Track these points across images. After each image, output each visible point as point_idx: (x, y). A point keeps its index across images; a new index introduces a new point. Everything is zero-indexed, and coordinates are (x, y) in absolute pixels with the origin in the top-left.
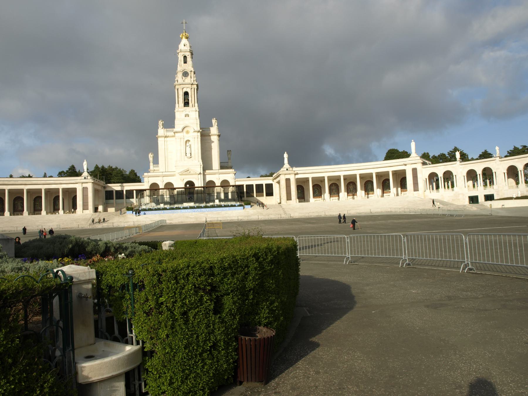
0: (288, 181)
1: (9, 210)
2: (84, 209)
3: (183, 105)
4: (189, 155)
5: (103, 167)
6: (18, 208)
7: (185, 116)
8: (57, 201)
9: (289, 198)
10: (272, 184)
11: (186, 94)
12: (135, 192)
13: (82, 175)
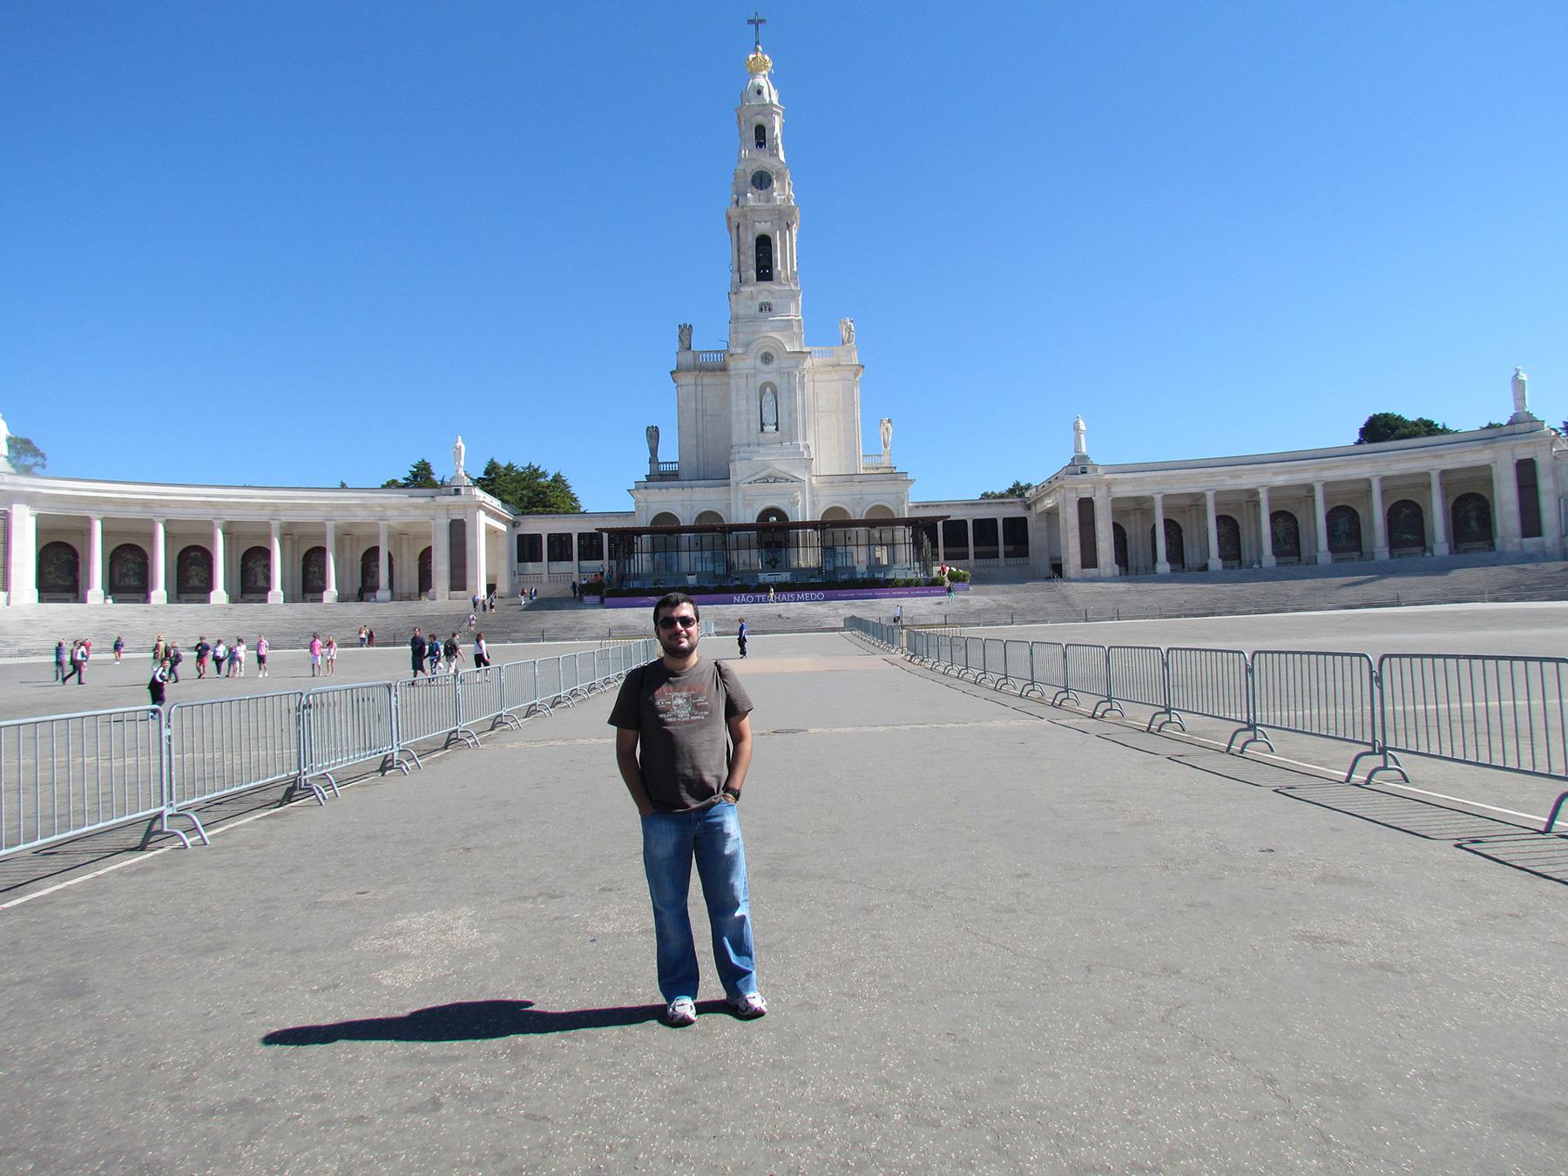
0: (1086, 507)
1: (228, 588)
3: (753, 273)
6: (256, 582)
7: (758, 307)
8: (374, 564)
9: (1089, 557)
10: (1024, 520)
12: (605, 535)
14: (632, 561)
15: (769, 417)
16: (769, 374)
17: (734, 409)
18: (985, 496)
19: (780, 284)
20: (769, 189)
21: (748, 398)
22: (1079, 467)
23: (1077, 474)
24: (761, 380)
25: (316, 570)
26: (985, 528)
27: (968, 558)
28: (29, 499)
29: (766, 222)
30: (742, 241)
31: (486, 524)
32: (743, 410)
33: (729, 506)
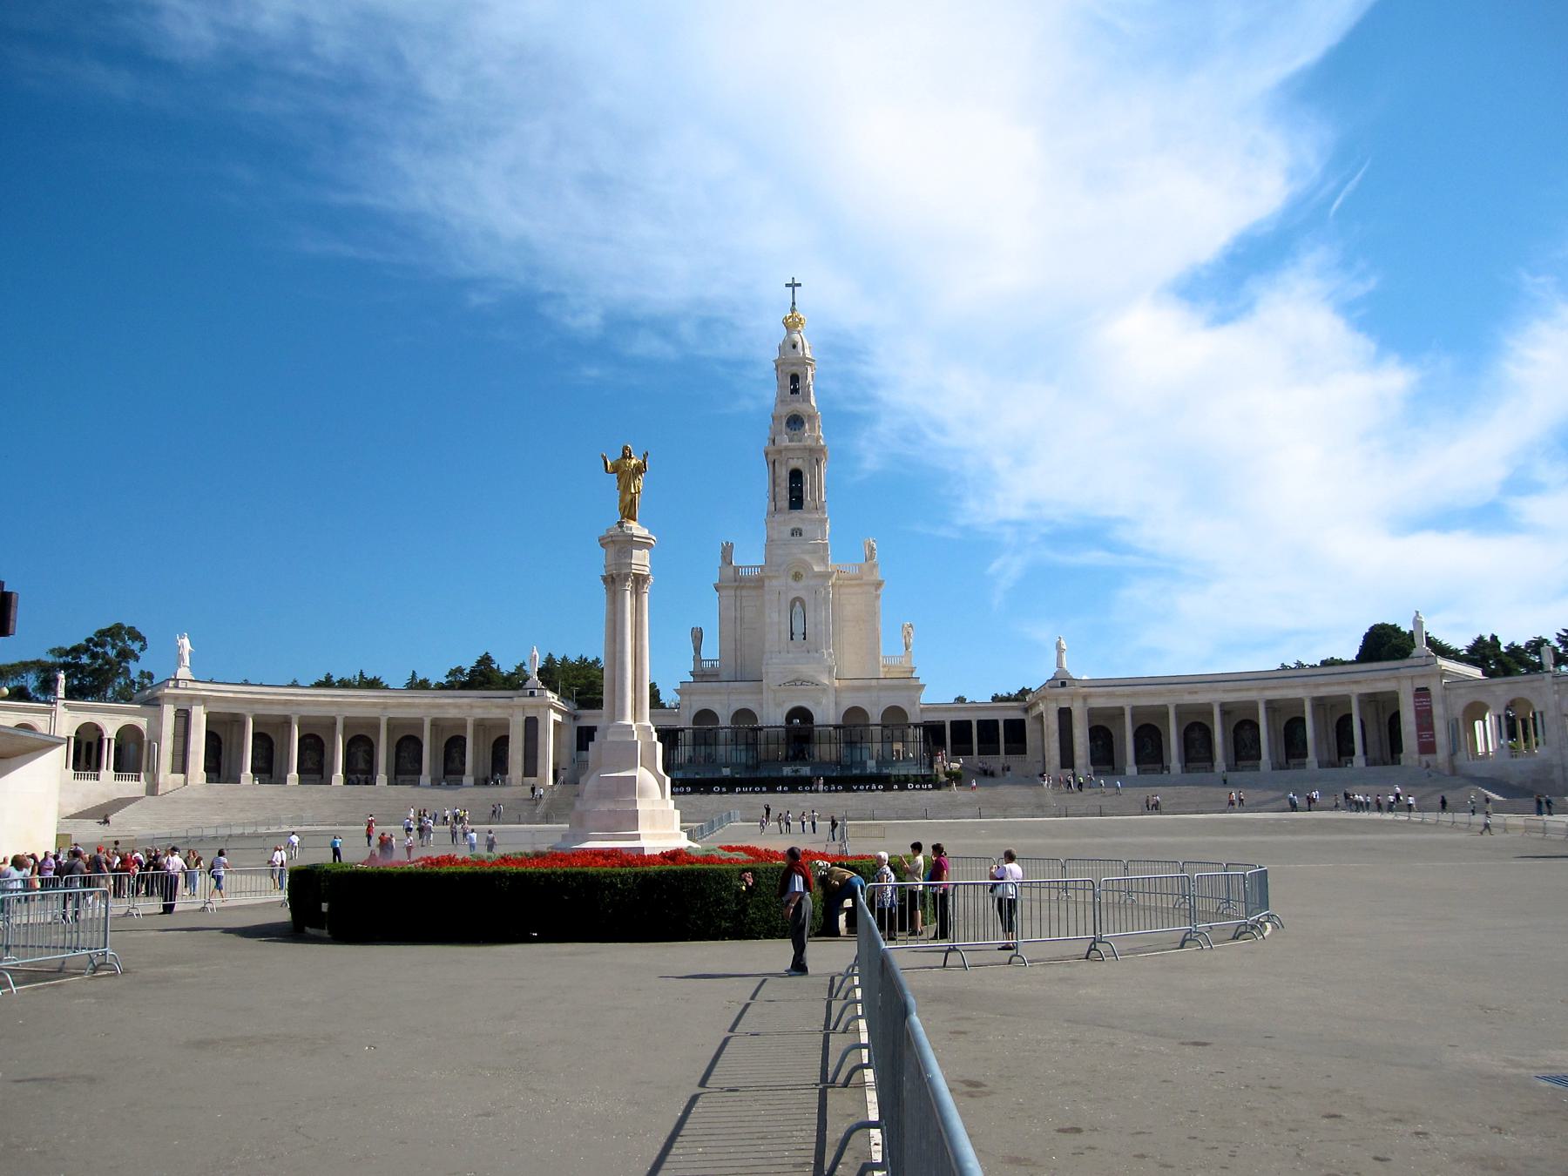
0: (1065, 715)
2: (526, 774)
3: (786, 504)
4: (798, 637)
5: (565, 659)
6: (357, 764)
7: (790, 532)
9: (1067, 760)
10: (1022, 722)
11: (796, 476)
13: (524, 687)
14: (676, 752)
15: (798, 629)
16: (798, 590)
17: (768, 620)
18: (995, 699)
19: (809, 512)
20: (802, 430)
21: (779, 611)
22: (1059, 681)
23: (1058, 687)
24: (793, 595)
25: (406, 755)
26: (988, 727)
27: (972, 754)
28: (204, 700)
29: (798, 458)
30: (777, 475)
31: (554, 720)
32: (776, 619)
33: (761, 705)
